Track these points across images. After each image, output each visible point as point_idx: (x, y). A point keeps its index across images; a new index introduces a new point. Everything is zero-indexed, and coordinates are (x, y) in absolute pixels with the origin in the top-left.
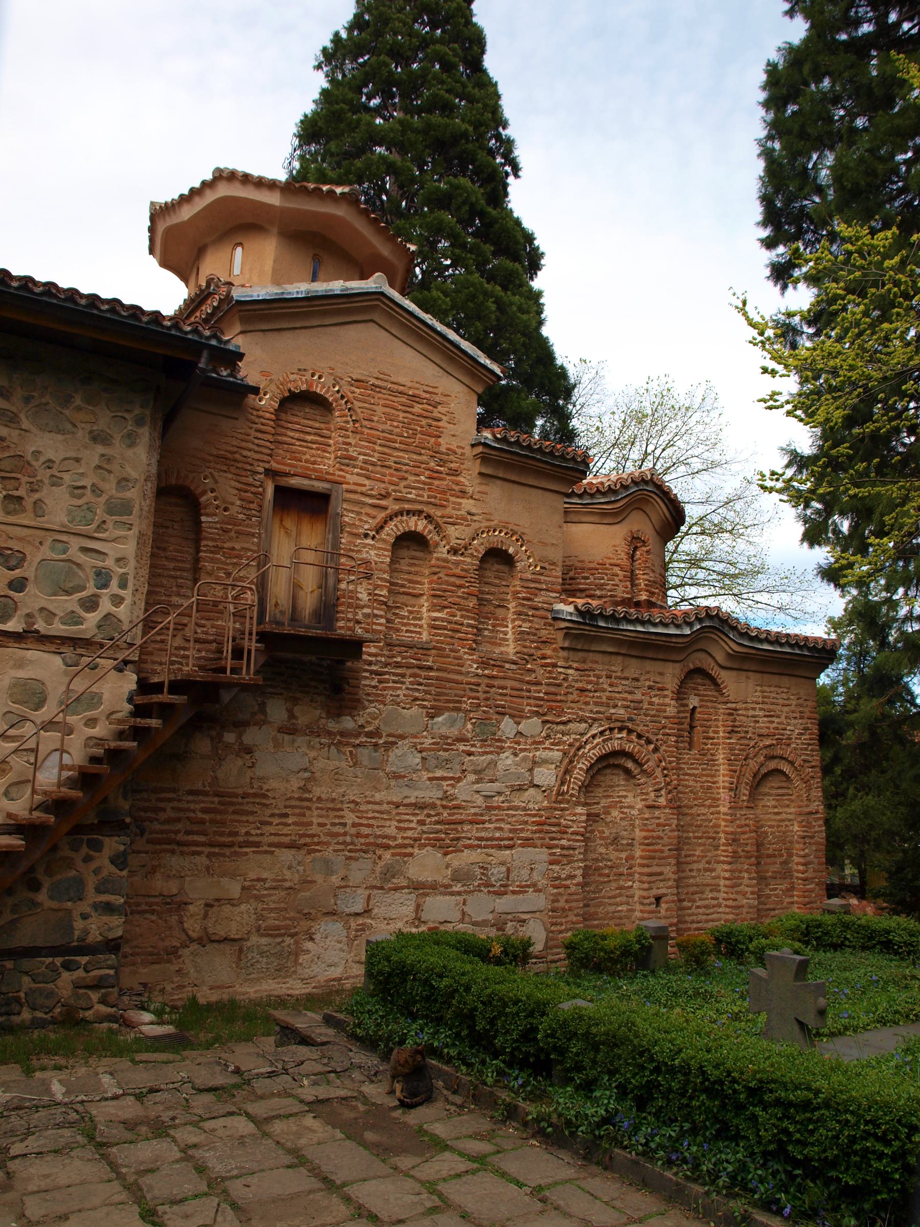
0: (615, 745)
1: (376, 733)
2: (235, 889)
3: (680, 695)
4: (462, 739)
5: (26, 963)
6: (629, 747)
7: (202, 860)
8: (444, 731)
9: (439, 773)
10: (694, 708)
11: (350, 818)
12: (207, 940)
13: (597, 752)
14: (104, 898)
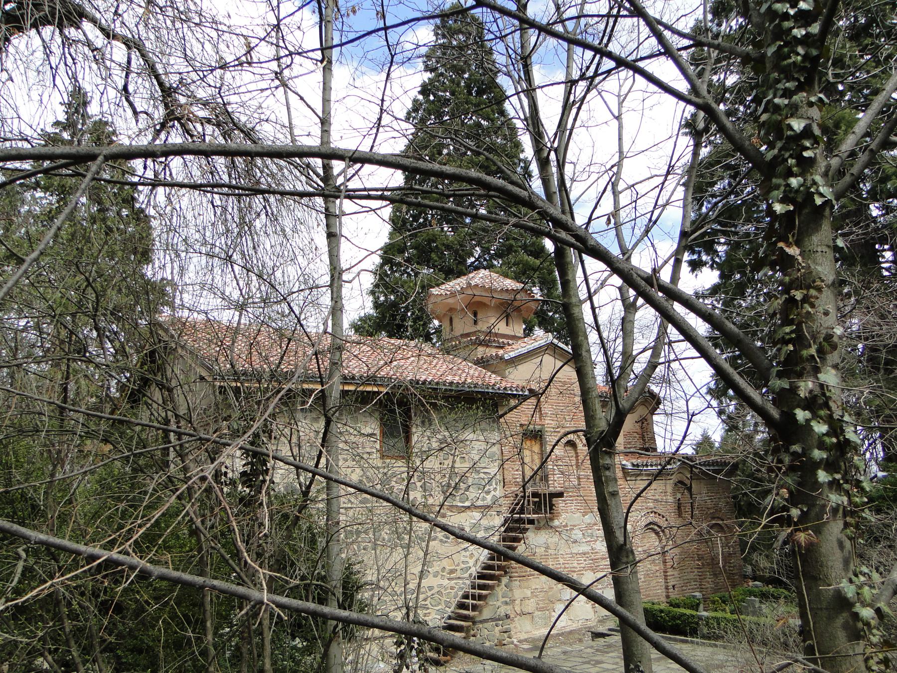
0: (650, 520)
1: (566, 526)
2: (528, 593)
3: (674, 494)
4: (595, 524)
5: (486, 625)
6: (656, 520)
7: (517, 583)
8: (589, 521)
9: (589, 539)
10: (679, 500)
11: (562, 561)
12: (523, 614)
13: (644, 524)
14: (504, 599)
